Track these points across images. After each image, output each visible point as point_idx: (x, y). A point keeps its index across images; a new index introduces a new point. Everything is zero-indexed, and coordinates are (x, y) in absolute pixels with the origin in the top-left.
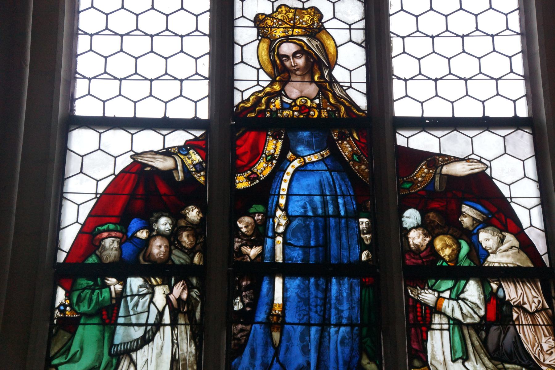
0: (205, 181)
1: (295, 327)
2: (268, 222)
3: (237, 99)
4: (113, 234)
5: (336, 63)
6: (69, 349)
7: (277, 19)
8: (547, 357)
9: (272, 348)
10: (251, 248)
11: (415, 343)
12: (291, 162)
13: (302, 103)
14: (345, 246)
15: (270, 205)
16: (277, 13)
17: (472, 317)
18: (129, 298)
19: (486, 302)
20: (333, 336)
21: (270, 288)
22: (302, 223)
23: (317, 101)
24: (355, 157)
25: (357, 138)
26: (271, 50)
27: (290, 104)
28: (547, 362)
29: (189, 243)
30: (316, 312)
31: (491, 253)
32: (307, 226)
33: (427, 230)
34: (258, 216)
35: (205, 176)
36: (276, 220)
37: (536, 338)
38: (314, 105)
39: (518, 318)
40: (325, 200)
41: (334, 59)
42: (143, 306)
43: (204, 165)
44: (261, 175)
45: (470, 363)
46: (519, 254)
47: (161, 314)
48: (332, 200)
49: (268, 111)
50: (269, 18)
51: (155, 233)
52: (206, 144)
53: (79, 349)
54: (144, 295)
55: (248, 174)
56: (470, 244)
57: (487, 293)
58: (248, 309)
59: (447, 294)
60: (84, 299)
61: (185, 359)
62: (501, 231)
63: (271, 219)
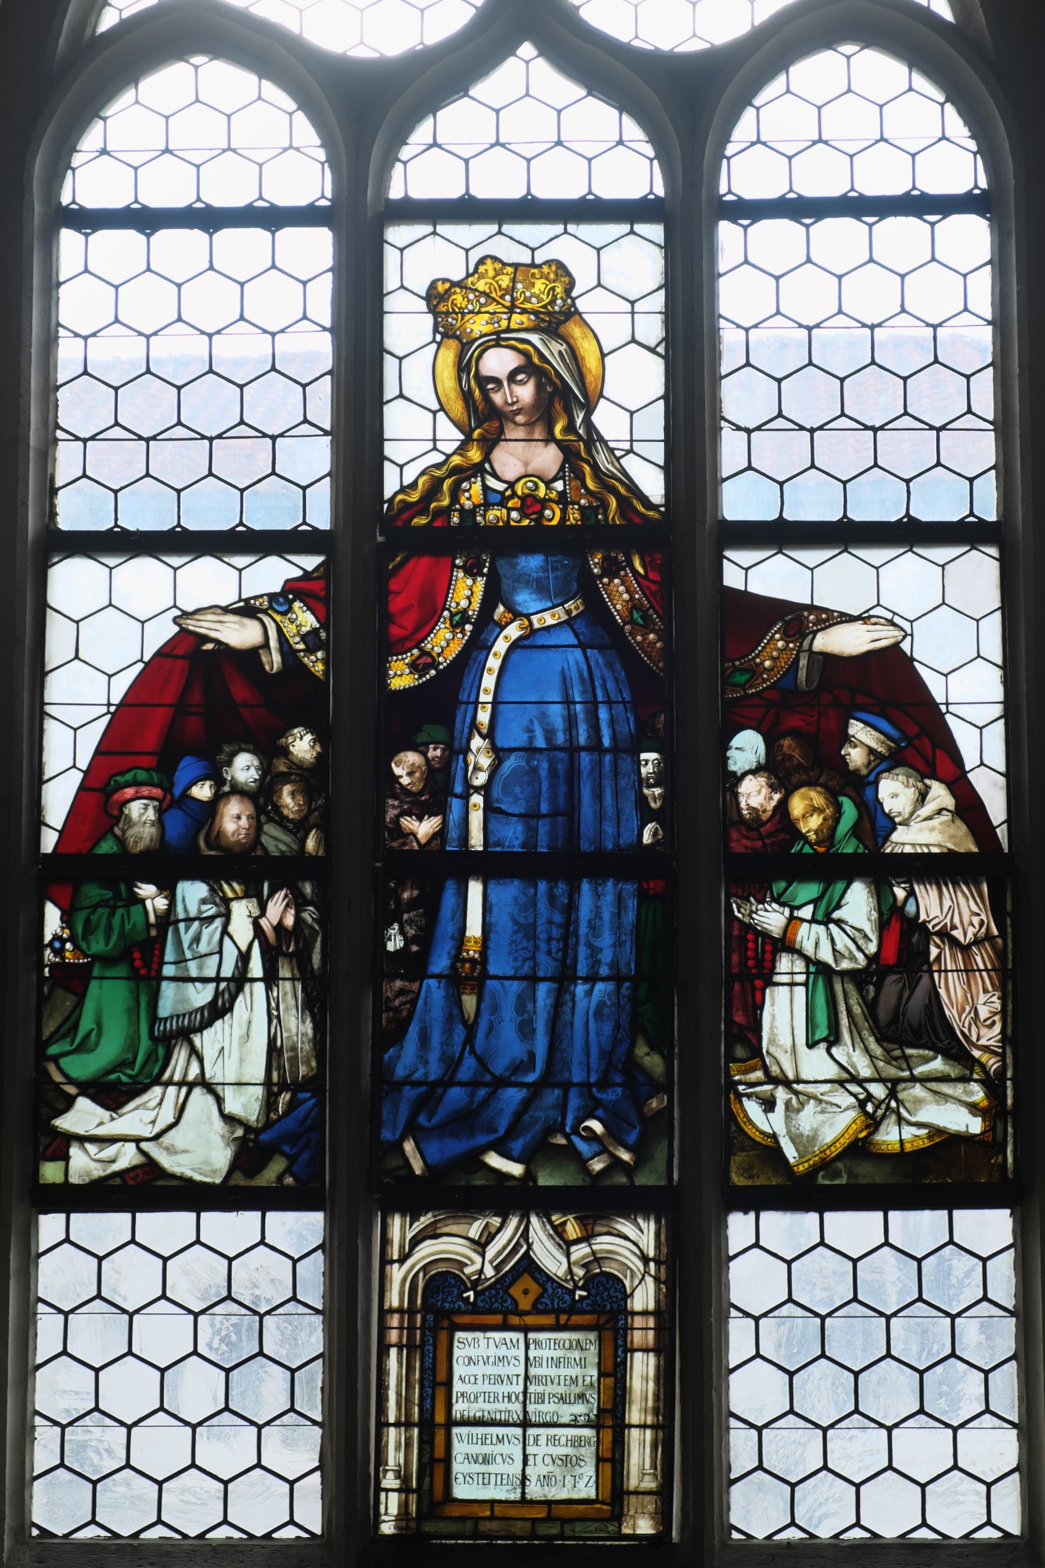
0: (326, 673)
1: (507, 983)
2: (454, 764)
3: (391, 485)
4: (145, 790)
5: (601, 395)
6: (76, 1027)
7: (476, 290)
8: (984, 1031)
9: (461, 1026)
10: (420, 819)
11: (740, 1013)
12: (503, 628)
13: (527, 491)
14: (610, 814)
15: (458, 725)
16: (476, 276)
17: (853, 958)
18: (182, 926)
19: (883, 926)
20: (582, 1000)
21: (458, 905)
22: (524, 764)
23: (559, 485)
24: (636, 615)
25: (641, 571)
26: (462, 367)
27: (502, 493)
28: (983, 1042)
29: (296, 808)
30: (549, 953)
31: (900, 824)
32: (534, 770)
33: (777, 777)
34: (435, 749)
35: (326, 661)
36: (471, 758)
37: (969, 996)
38: (553, 495)
39: (938, 958)
40: (572, 712)
41: (596, 386)
42: (209, 943)
43: (323, 635)
44: (441, 659)
45: (841, 1048)
46: (953, 826)
47: (244, 958)
48: (587, 713)
49: (456, 510)
50: (458, 290)
51: (226, 789)
52: (327, 588)
53: (95, 1026)
54: (211, 919)
55: (414, 657)
56: (860, 805)
57: (885, 908)
58: (415, 948)
59: (806, 912)
60: (97, 927)
61: (294, 1049)
62: (923, 776)
63: (461, 757)
